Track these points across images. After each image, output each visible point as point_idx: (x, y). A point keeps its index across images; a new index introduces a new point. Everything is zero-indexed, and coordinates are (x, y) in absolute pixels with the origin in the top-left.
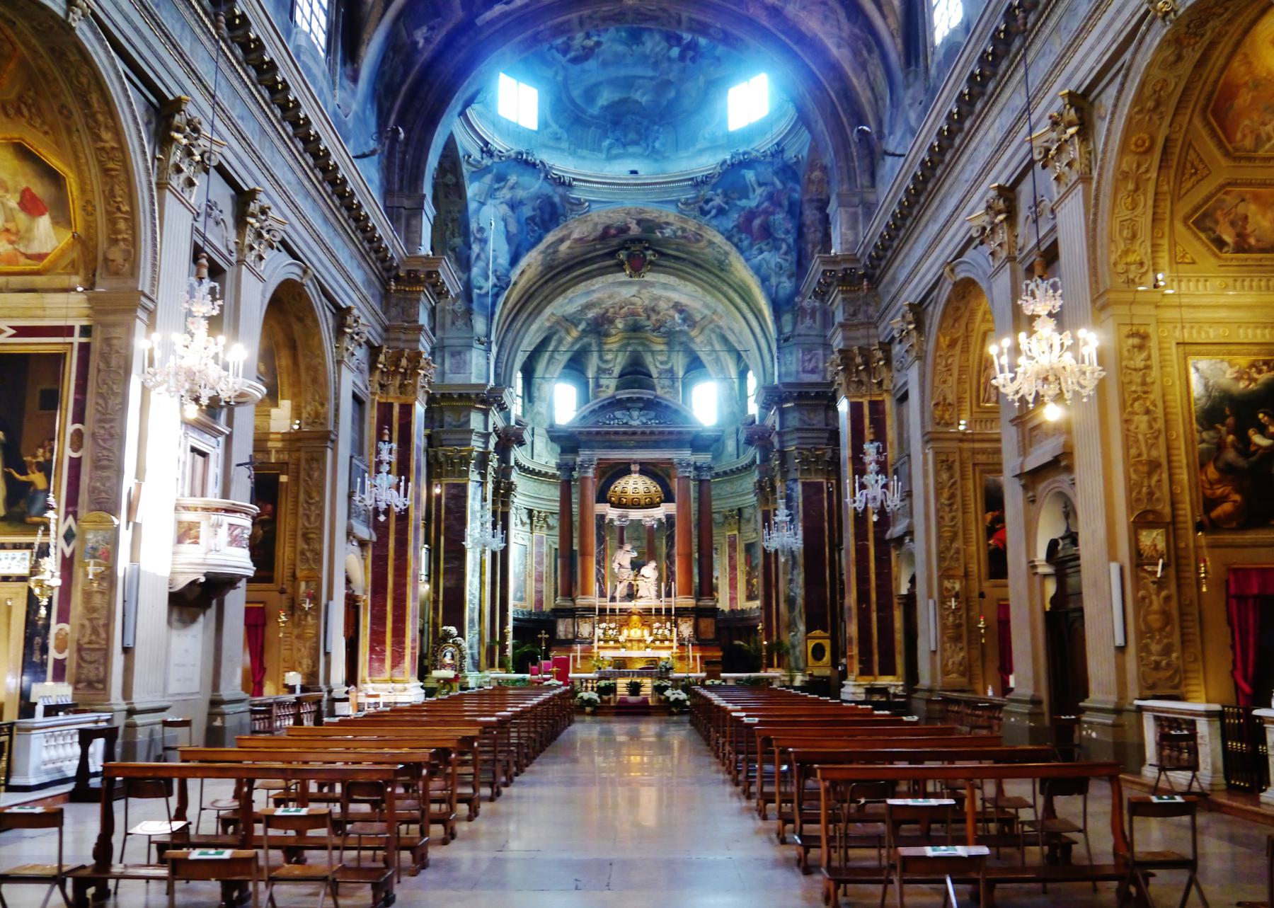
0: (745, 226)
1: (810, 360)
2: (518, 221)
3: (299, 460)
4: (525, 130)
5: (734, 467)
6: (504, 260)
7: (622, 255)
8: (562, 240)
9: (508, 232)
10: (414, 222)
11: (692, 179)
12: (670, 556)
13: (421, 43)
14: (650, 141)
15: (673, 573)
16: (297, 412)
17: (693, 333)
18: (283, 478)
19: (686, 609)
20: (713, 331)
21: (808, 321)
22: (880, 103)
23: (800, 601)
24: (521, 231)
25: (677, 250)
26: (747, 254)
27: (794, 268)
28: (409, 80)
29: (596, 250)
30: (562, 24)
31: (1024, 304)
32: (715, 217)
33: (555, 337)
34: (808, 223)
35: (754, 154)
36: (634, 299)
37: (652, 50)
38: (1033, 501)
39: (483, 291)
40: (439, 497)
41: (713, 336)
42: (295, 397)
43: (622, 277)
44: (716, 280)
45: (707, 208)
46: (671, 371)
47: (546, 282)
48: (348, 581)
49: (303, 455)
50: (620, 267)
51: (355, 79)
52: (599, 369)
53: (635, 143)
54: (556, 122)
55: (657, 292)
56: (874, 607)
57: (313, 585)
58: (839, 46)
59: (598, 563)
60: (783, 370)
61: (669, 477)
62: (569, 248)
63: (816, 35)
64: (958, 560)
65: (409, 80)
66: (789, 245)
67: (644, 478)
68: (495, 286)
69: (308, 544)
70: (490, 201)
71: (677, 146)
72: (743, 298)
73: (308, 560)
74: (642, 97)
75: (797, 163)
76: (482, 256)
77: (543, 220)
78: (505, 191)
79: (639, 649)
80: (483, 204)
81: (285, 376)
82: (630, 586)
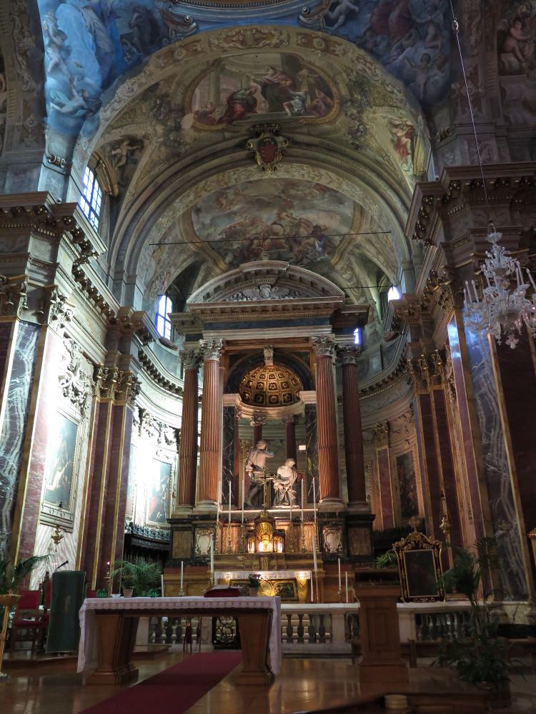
2: (111, 37)
5: (380, 381)
6: (93, 79)
7: (252, 144)
9: (98, 48)
20: (352, 253)
25: (309, 134)
29: (224, 140)
33: (203, 267)
39: (64, 110)
41: (353, 259)
44: (351, 162)
45: (333, 15)
50: (251, 158)
59: (225, 463)
66: (437, 26)
68: (82, 107)
72: (380, 176)
76: (64, 67)
79: (270, 568)
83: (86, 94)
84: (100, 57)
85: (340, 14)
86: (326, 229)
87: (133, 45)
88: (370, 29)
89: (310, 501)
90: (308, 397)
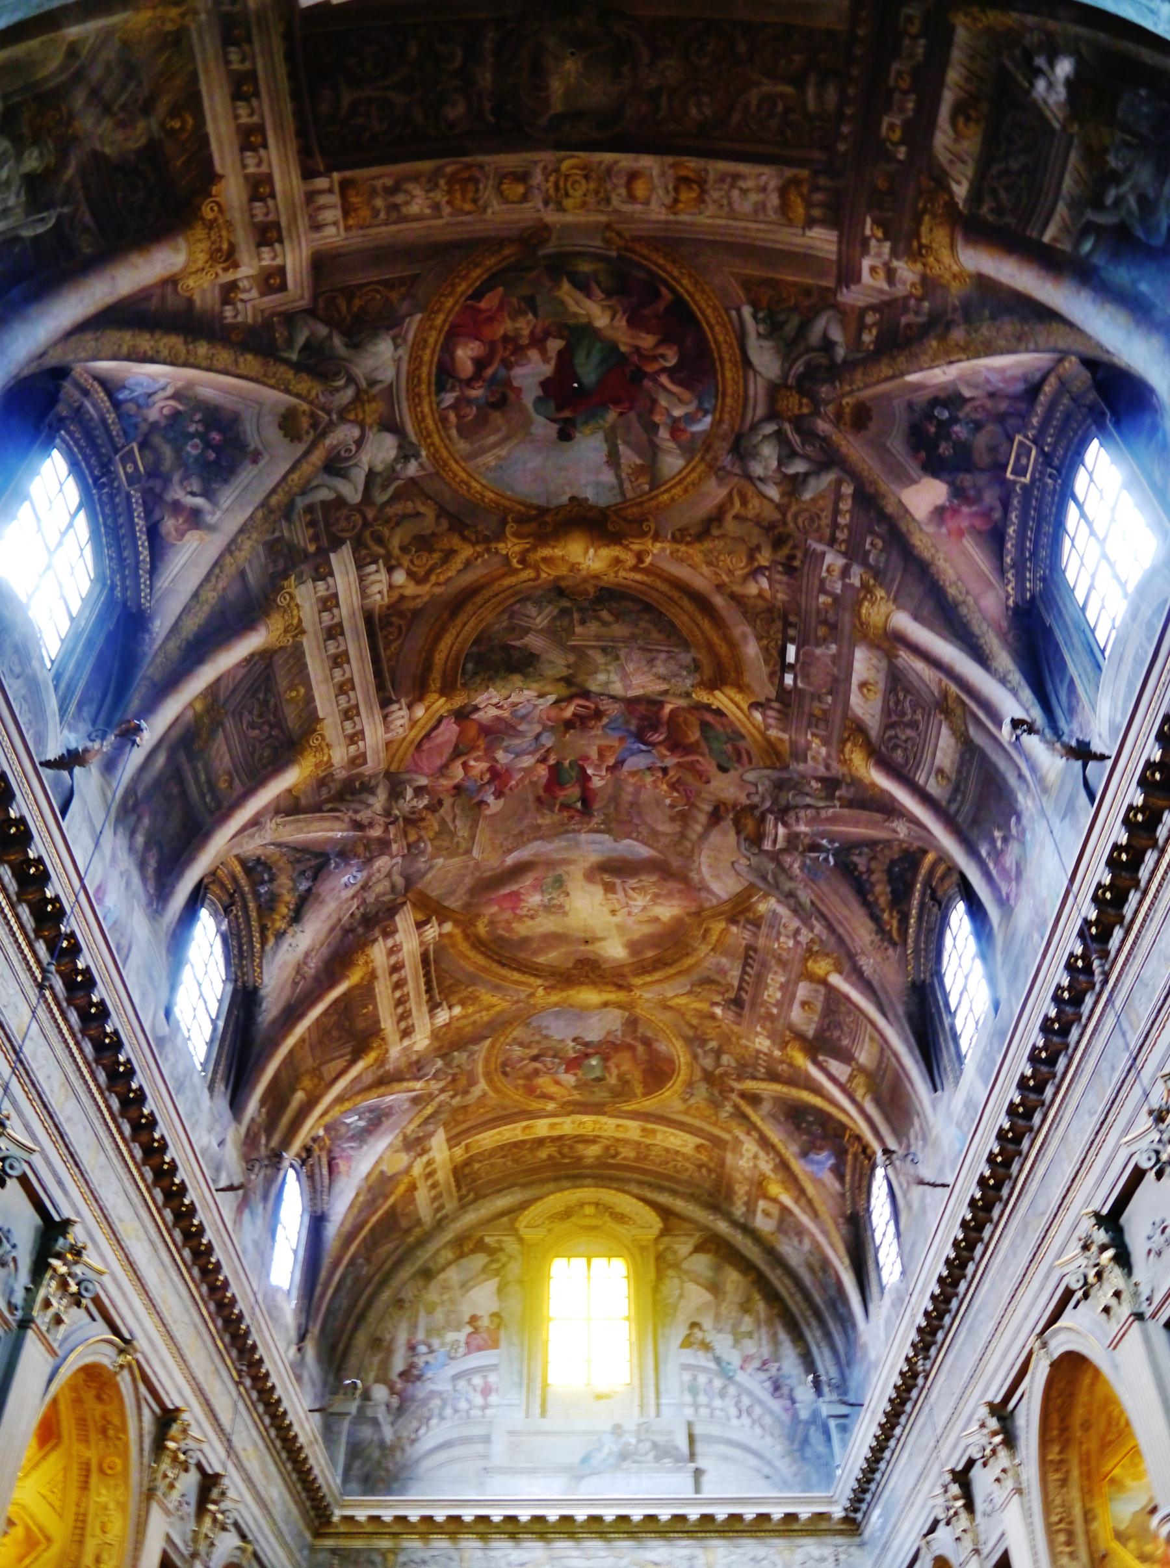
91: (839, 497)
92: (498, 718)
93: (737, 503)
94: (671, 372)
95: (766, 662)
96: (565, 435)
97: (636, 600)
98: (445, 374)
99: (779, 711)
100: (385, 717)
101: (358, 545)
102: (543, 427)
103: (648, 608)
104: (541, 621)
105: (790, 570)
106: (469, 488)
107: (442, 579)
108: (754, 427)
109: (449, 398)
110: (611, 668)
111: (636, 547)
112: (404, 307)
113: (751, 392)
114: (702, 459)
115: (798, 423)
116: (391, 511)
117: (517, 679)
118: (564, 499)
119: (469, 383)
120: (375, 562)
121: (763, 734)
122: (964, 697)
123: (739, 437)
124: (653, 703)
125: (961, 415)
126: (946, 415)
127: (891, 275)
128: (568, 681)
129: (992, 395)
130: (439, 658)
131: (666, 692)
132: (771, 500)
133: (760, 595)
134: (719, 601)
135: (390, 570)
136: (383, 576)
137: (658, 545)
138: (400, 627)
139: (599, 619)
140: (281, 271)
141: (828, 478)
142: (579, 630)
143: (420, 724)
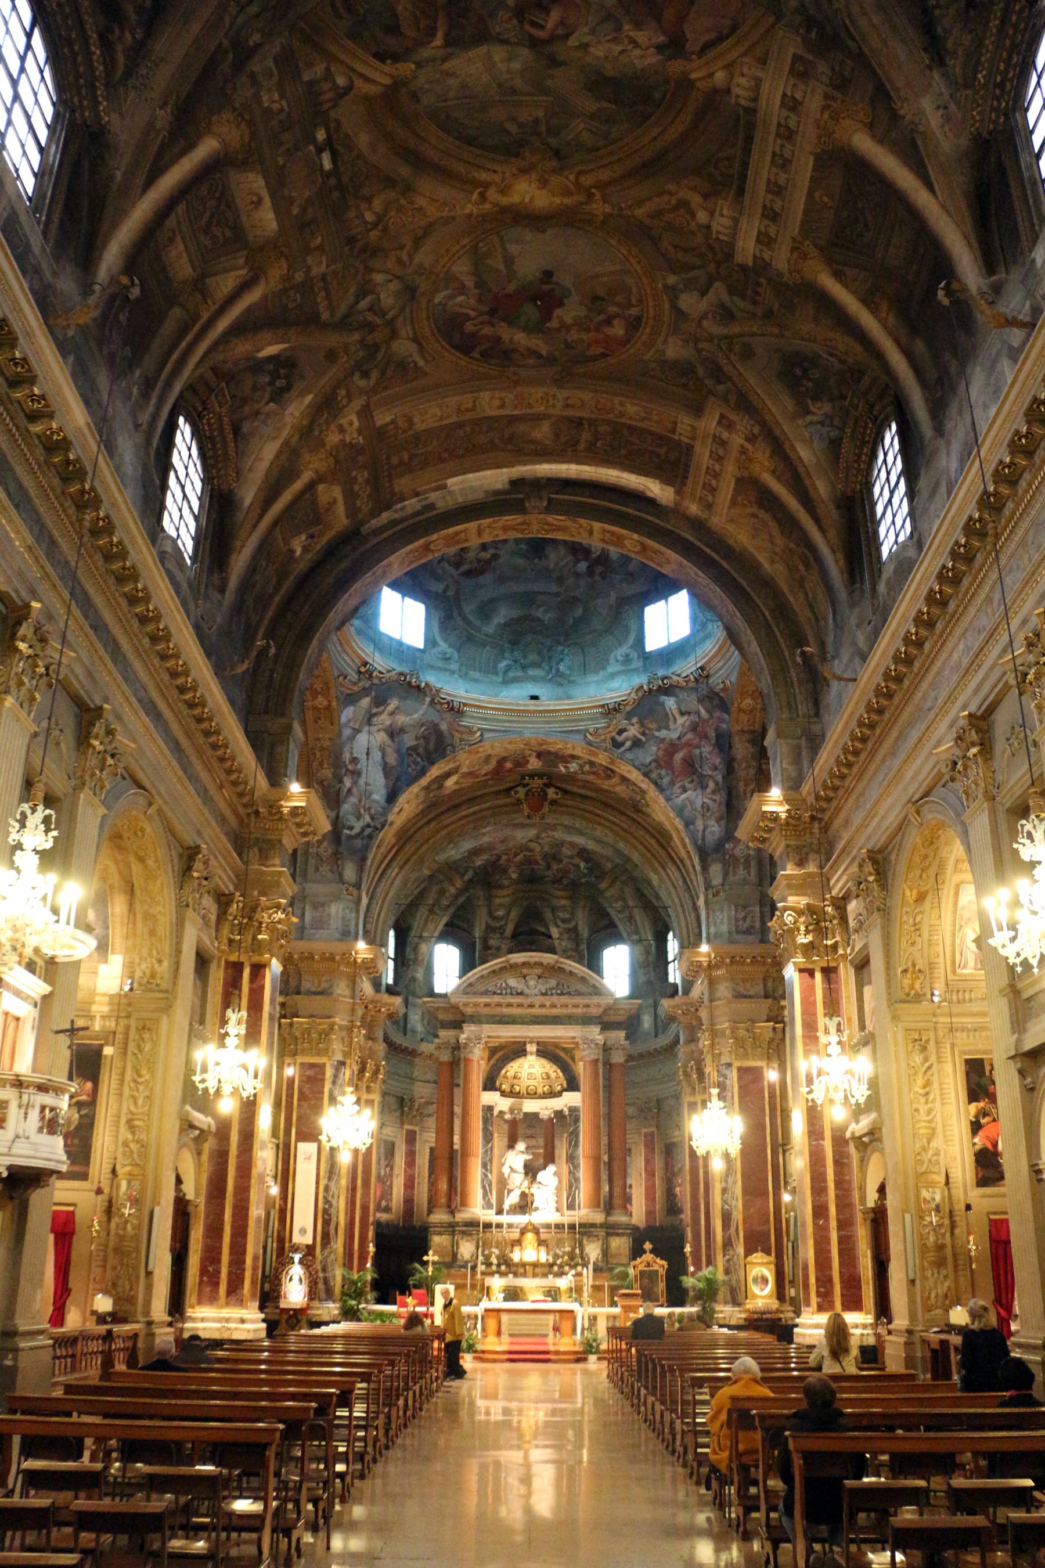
0: (664, 761)
1: (744, 919)
2: (398, 752)
3: (128, 1028)
4: (409, 648)
6: (379, 796)
7: (521, 792)
8: (447, 775)
10: (279, 749)
11: (603, 706)
12: (571, 1159)
13: (298, 551)
14: (554, 664)
15: (577, 1180)
16: (129, 970)
17: (603, 885)
18: (108, 1051)
19: (593, 1225)
21: (741, 872)
22: (822, 623)
23: (738, 1216)
24: (401, 762)
25: (584, 787)
26: (668, 792)
27: (723, 809)
28: (283, 591)
30: (457, 534)
31: (1020, 847)
32: (630, 749)
33: (435, 889)
34: (739, 757)
35: (675, 678)
36: (532, 845)
37: (557, 564)
38: (1032, 1089)
40: (291, 1081)
42: (127, 951)
43: (519, 819)
45: (620, 739)
46: (575, 930)
47: (429, 822)
48: (179, 1181)
49: (133, 1023)
51: (222, 590)
52: (488, 926)
53: (537, 665)
54: (445, 641)
55: (559, 835)
56: (833, 1224)
57: (136, 1184)
58: (772, 562)
59: (484, 1166)
60: (712, 930)
61: (573, 1059)
62: (456, 783)
63: (745, 549)
64: (938, 1163)
65: (283, 591)
66: (717, 784)
67: (544, 1062)
68: (368, 826)
69: (133, 1133)
70: (366, 728)
71: (584, 669)
73: (132, 1152)
74: (546, 616)
75: (725, 689)
76: (355, 790)
77: (427, 752)
78: (384, 717)
79: (535, 1275)
80: (358, 731)
81: (118, 926)
82: (523, 1195)
83: (373, 811)
84: (386, 769)
85: (627, 739)
86: (595, 853)
87: (418, 755)
88: (654, 761)
89: (571, 1207)
90: (571, 1099)
91: (332, 308)
92: (638, 25)
93: (405, 258)
94: (468, 318)
95: (348, 136)
96: (548, 275)
97: (482, 147)
98: (635, 324)
99: (321, 103)
100: (755, 99)
101: (729, 256)
102: (566, 281)
103: (471, 141)
104: (579, 126)
105: (351, 240)
106: (629, 251)
107: (666, 197)
108: (402, 309)
109: (634, 311)
110: (505, 76)
111: (488, 206)
112: (653, 365)
113: (409, 328)
114: (438, 275)
115: (371, 327)
116: (698, 262)
117: (610, 71)
118: (550, 232)
119: (618, 316)
120: (717, 239)
121: (332, 58)
122: (197, 328)
123: (412, 298)
124: (455, 42)
125: (269, 389)
126: (278, 384)
127: (341, 429)
128: (554, 62)
129: (257, 413)
130: (687, 117)
131: (444, 60)
132: (378, 272)
133: (369, 200)
134: (405, 171)
135: (708, 227)
136: (715, 227)
137: (467, 211)
138: (716, 167)
139: (520, 125)
140: (719, 423)
141: (343, 308)
142: (540, 114)
143: (721, 63)
